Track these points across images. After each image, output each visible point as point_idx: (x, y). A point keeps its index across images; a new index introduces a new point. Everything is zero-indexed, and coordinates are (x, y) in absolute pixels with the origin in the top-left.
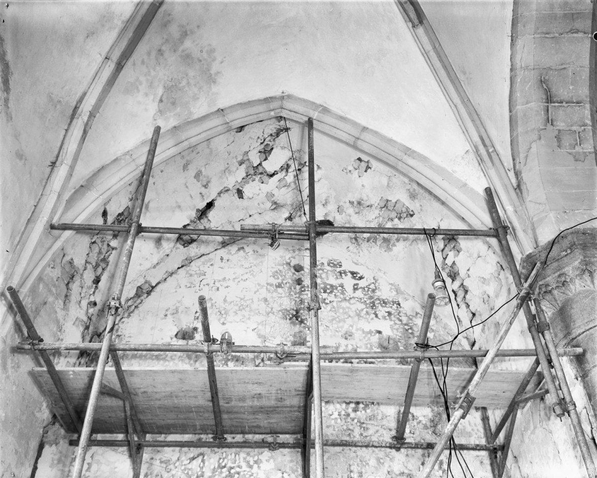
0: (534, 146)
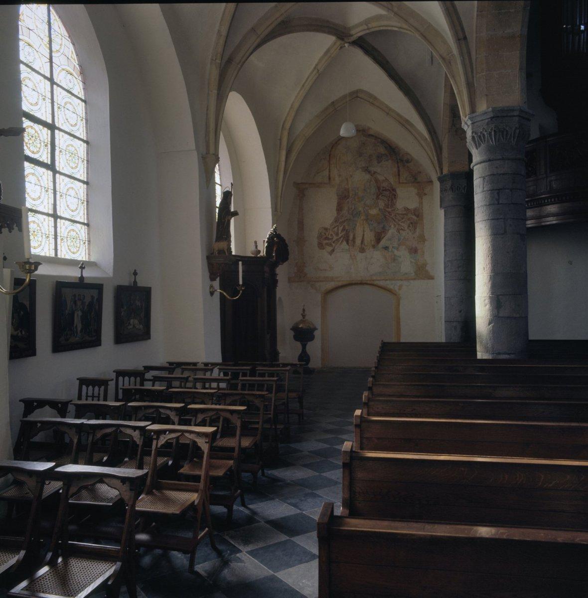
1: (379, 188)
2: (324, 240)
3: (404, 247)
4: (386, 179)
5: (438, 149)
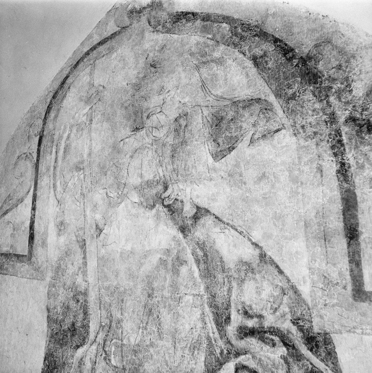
1: (222, 320)
4: (263, 256)
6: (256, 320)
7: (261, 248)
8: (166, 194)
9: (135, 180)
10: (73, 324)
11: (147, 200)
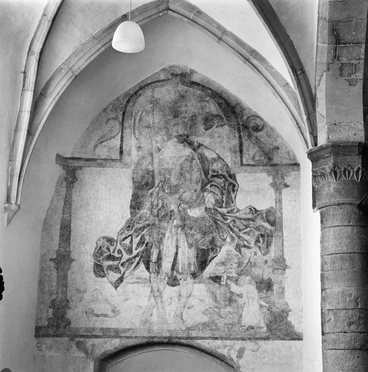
0: (325, 74)
1: (206, 174)
2: (106, 260)
3: (248, 278)
4: (219, 157)
5: (310, 101)
6: (216, 173)
7: (218, 155)
8: (188, 139)
9: (175, 134)
10: (147, 182)
11: (180, 141)
